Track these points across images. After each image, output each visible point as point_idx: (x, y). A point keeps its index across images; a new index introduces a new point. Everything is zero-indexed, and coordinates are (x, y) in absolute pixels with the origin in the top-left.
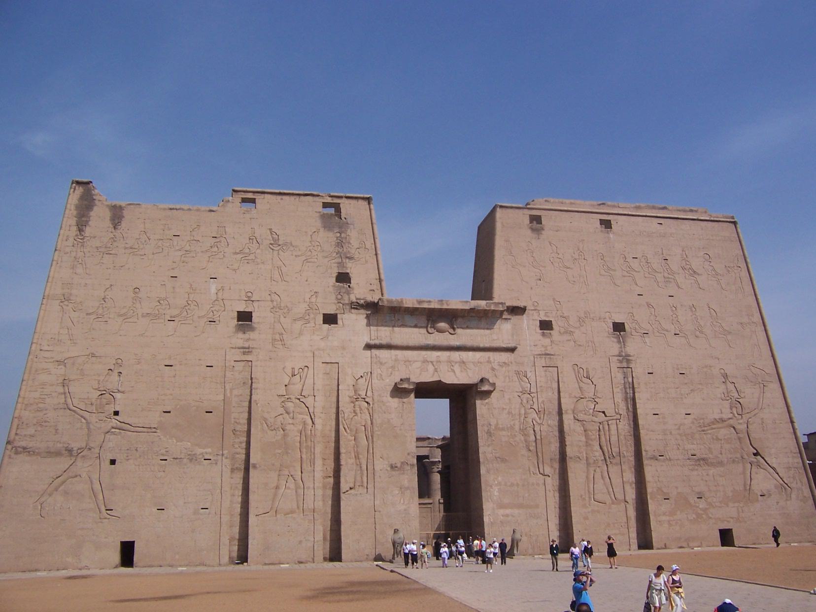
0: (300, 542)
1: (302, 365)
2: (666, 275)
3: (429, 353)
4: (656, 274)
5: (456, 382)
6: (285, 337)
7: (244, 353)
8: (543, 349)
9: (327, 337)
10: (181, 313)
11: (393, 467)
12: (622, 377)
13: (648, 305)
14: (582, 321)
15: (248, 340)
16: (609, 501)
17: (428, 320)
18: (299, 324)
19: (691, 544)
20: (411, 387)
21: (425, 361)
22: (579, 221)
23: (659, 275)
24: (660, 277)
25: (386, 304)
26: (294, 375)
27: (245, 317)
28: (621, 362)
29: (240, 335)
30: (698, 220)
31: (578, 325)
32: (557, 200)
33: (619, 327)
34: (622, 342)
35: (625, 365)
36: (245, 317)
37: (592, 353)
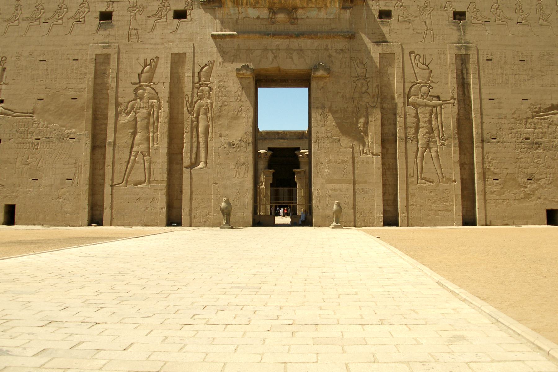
0: (147, 208)
1: (153, 56)
6: (139, 32)
7: (104, 47)
8: (381, 37)
9: (176, 30)
10: (54, 16)
11: (231, 145)
12: (460, 64)
14: (422, 9)
15: (108, 36)
16: (436, 180)
17: (270, 12)
18: (151, 21)
19: (516, 222)
21: (265, 49)
26: (146, 66)
27: (106, 16)
28: (459, 49)
29: (101, 32)
33: (459, 16)
34: (463, 30)
35: (463, 52)
36: (106, 16)
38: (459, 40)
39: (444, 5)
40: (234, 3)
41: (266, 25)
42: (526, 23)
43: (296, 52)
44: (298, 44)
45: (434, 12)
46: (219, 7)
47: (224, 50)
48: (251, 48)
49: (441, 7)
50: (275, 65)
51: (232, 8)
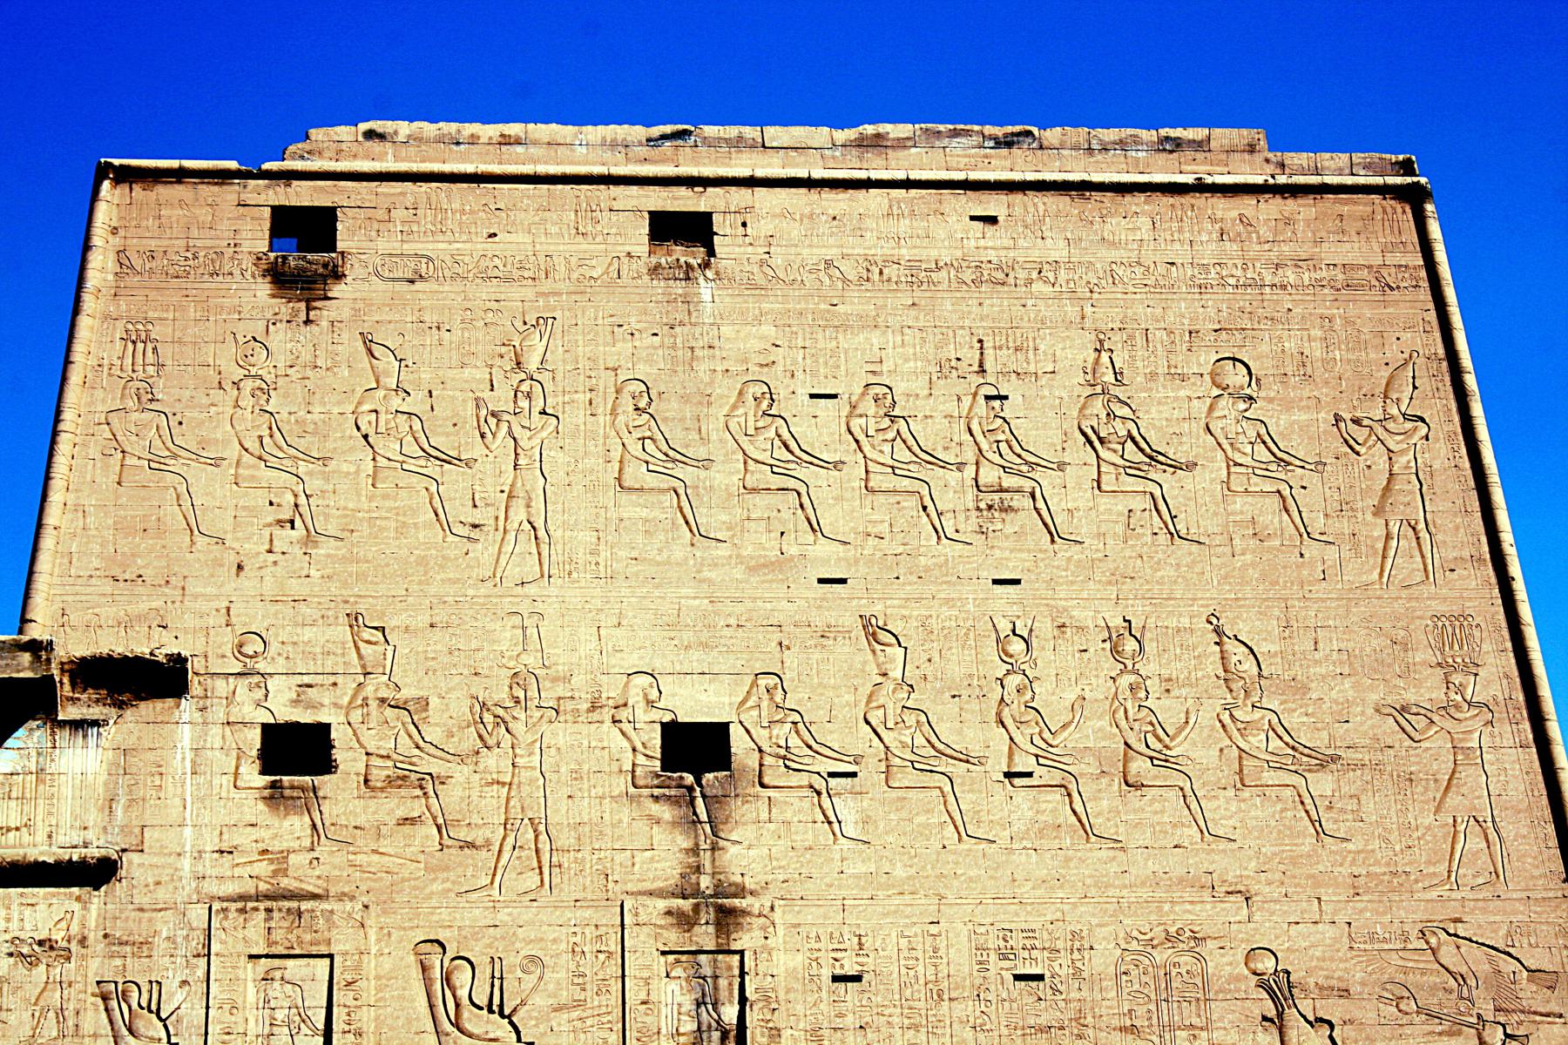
2: (989, 475)
4: (935, 475)
8: (263, 869)
12: (689, 1005)
13: (873, 631)
14: (489, 721)
22: (536, 227)
23: (953, 477)
24: (952, 491)
28: (685, 922)
30: (1200, 187)
31: (470, 740)
32: (429, 129)
33: (695, 749)
34: (706, 824)
37: (532, 880)
38: (683, 876)
39: (612, 692)
42: (1057, 778)
45: (560, 735)
49: (594, 708)
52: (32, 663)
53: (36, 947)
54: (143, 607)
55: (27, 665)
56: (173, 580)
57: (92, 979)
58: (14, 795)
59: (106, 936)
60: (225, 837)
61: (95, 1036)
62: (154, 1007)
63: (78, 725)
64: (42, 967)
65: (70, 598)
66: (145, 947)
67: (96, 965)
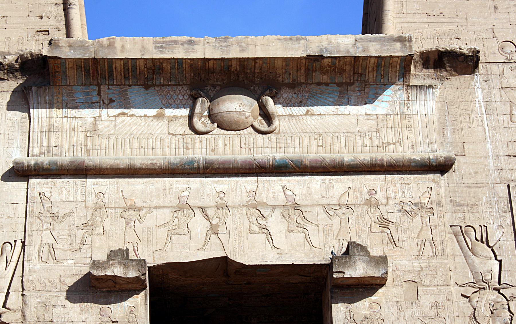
3: (195, 182)
5: (271, 258)
20: (132, 274)
21: (184, 207)
25: (66, 53)
40: (87, 72)
41: (183, 135)
43: (278, 212)
44: (284, 188)
46: (39, 87)
47: (54, 210)
48: (139, 204)
50: (212, 252)
51: (79, 88)
52: (401, 48)
53: (413, 207)
54: (446, 28)
55: (399, 49)
56: (460, 15)
57: (448, 225)
58: (389, 126)
59: (451, 201)
60: (510, 148)
61: (454, 256)
62: (484, 240)
63: (420, 87)
64: (419, 218)
65: (405, 25)
66: (474, 207)
67: (449, 218)
